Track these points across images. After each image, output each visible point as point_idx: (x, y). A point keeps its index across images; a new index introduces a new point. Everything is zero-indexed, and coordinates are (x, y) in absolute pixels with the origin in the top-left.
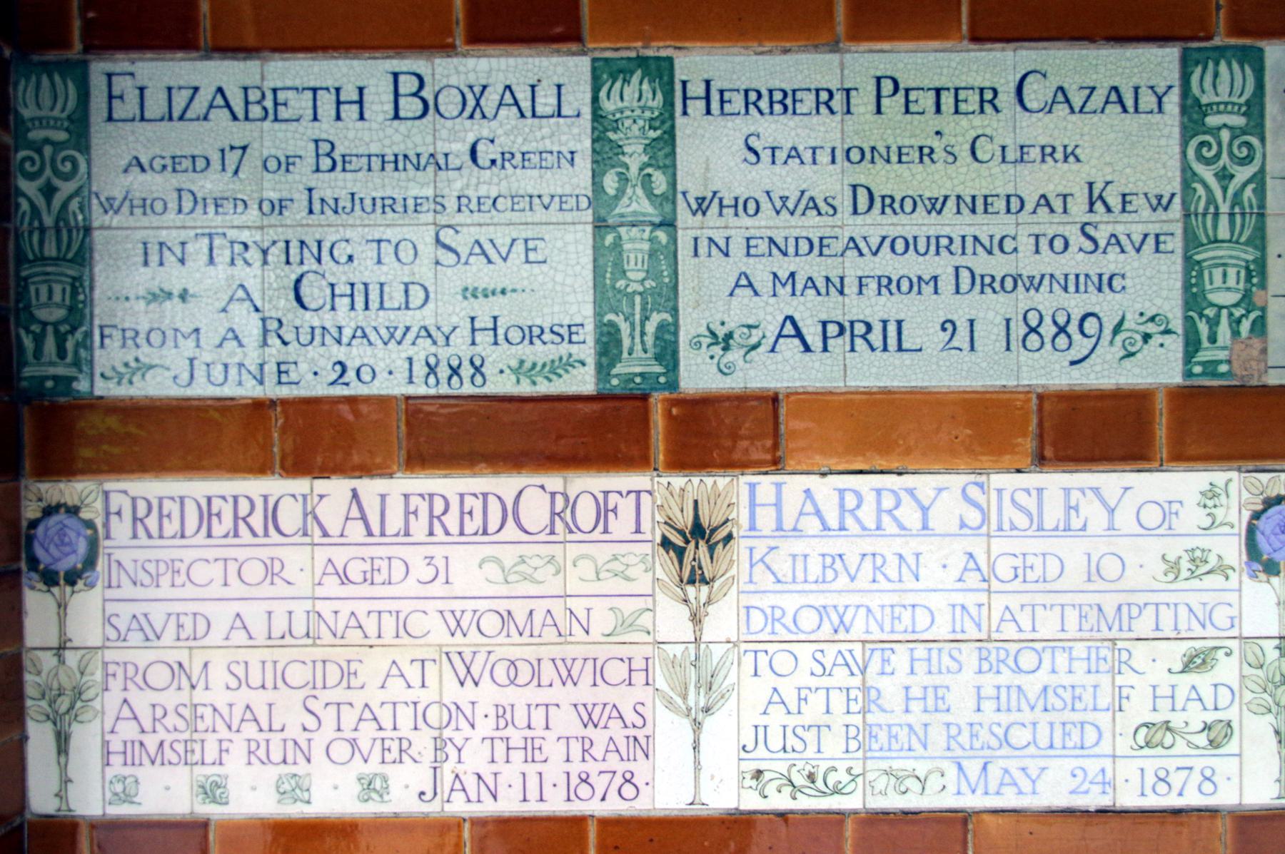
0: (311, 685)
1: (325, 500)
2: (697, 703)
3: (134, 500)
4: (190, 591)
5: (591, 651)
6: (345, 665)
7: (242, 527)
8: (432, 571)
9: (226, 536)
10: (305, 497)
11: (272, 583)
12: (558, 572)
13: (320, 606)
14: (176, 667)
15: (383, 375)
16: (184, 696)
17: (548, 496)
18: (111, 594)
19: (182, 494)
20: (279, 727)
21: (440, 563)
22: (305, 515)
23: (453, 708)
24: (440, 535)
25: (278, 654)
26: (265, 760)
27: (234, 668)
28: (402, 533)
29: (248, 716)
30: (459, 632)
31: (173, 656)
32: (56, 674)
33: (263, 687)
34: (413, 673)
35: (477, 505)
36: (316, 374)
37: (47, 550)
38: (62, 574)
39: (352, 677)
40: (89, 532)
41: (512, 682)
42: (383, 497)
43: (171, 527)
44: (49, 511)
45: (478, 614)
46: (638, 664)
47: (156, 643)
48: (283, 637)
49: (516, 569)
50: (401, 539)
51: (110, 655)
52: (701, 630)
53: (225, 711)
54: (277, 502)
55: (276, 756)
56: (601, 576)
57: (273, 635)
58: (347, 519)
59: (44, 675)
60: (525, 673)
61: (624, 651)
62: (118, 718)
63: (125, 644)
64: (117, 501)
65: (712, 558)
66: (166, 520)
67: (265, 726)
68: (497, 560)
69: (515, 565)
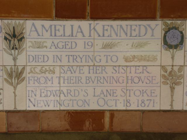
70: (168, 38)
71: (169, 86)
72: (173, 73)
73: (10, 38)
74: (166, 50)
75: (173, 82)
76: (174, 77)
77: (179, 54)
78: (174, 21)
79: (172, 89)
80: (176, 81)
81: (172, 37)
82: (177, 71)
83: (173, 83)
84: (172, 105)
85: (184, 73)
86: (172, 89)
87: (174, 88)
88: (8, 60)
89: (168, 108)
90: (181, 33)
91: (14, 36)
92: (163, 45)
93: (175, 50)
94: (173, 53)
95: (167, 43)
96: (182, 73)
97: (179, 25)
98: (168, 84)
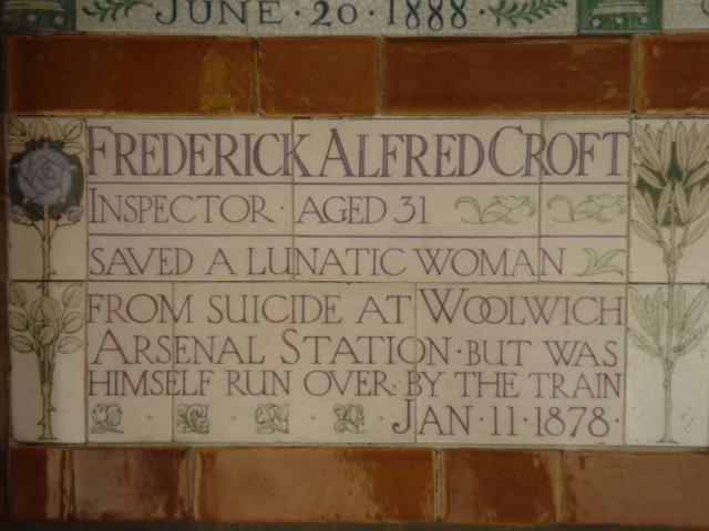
0: (290, 319)
1: (305, 139)
2: (669, 342)
3: (117, 136)
4: (172, 227)
5: (564, 290)
6: (323, 300)
7: (224, 163)
8: (407, 211)
9: (209, 174)
10: (286, 137)
11: (254, 221)
12: (532, 214)
13: (300, 243)
14: (159, 300)
15: (363, 16)
16: (167, 329)
17: (524, 138)
18: (94, 228)
19: (165, 131)
20: (259, 359)
21: (417, 203)
22: (286, 155)
23: (427, 343)
24: (418, 177)
25: (257, 288)
26: (244, 390)
27: (216, 301)
28: (381, 173)
29: (229, 348)
30: (434, 271)
31: (155, 290)
32: (40, 306)
33: (244, 320)
34: (389, 309)
35: (455, 146)
36: (297, 13)
37: (31, 185)
38: (46, 208)
39: (330, 312)
40: (73, 167)
41: (485, 319)
42: (362, 138)
43: (155, 164)
44: (33, 146)
45: (453, 253)
46: (611, 303)
47: (140, 277)
48: (263, 273)
49: (492, 209)
50: (378, 180)
51: (94, 288)
52: (674, 271)
53: (206, 343)
54: (259, 142)
55: (256, 388)
56: (575, 217)
57: (254, 271)
58: (327, 159)
59: (28, 306)
60: (498, 311)
61: (596, 291)
62: (101, 350)
63: (110, 278)
64: (101, 137)
65: (688, 200)
66: (149, 157)
67: (245, 358)
68: (473, 201)
69: (491, 205)
73: (655, 183)
88: (647, 263)
91: (675, 172)
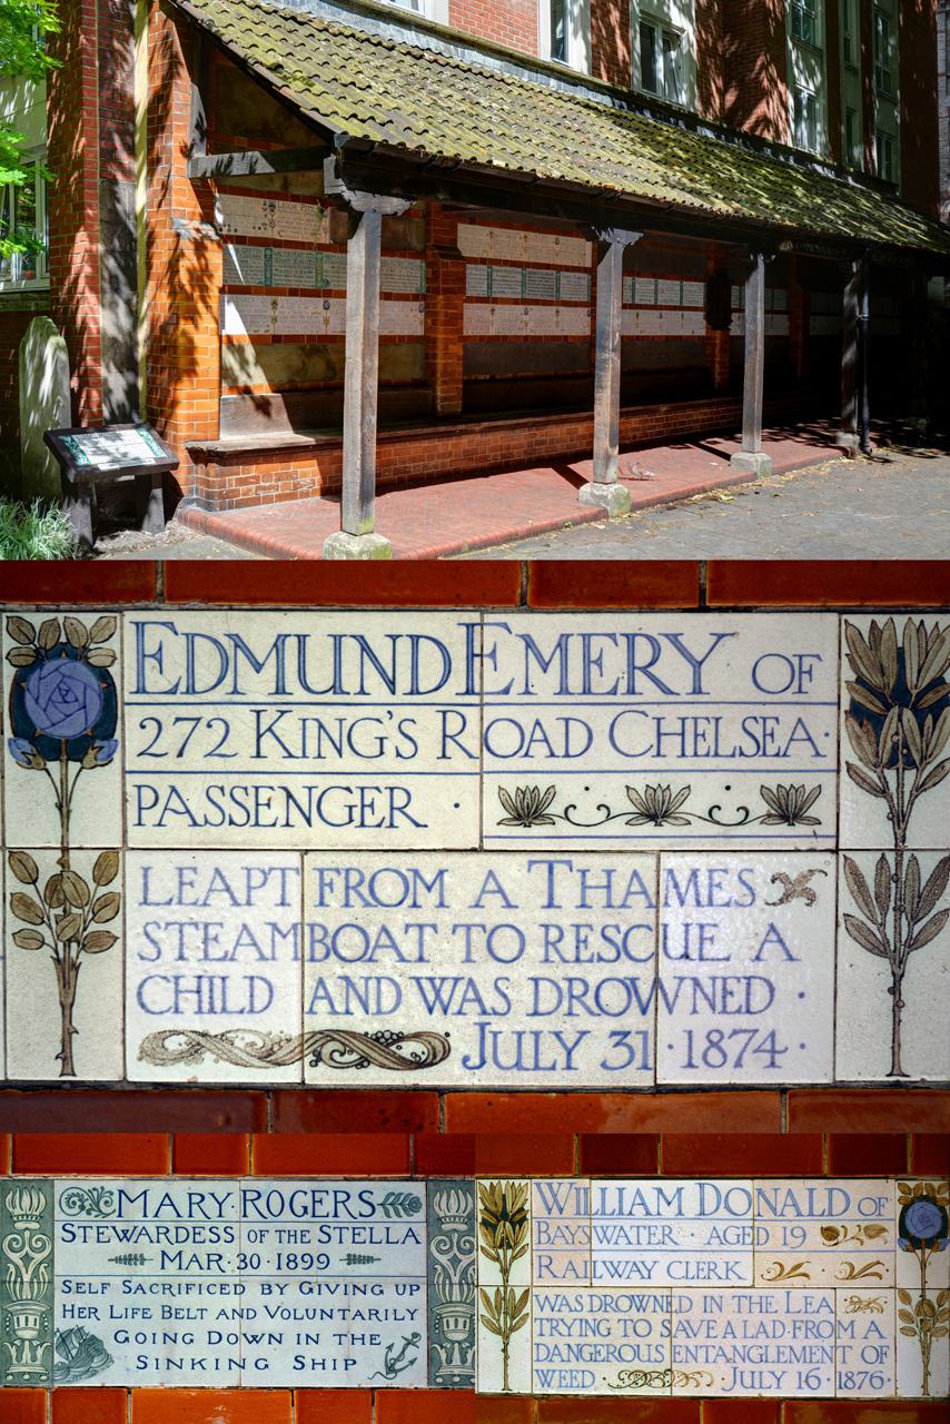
70: (37, 701)
71: (47, 952)
72: (67, 887)
74: (29, 765)
75: (69, 933)
76: (74, 910)
77: (97, 787)
78: (61, 617)
79: (67, 972)
80: (85, 929)
81: (57, 697)
82: (87, 875)
83: (69, 941)
84: (65, 1057)
85: (123, 885)
86: (67, 972)
87: (76, 967)
89: (51, 1072)
90: (103, 674)
92: (10, 740)
93: (74, 766)
94: (64, 780)
95: (32, 726)
96: (115, 886)
97: (90, 638)
98: (43, 943)
